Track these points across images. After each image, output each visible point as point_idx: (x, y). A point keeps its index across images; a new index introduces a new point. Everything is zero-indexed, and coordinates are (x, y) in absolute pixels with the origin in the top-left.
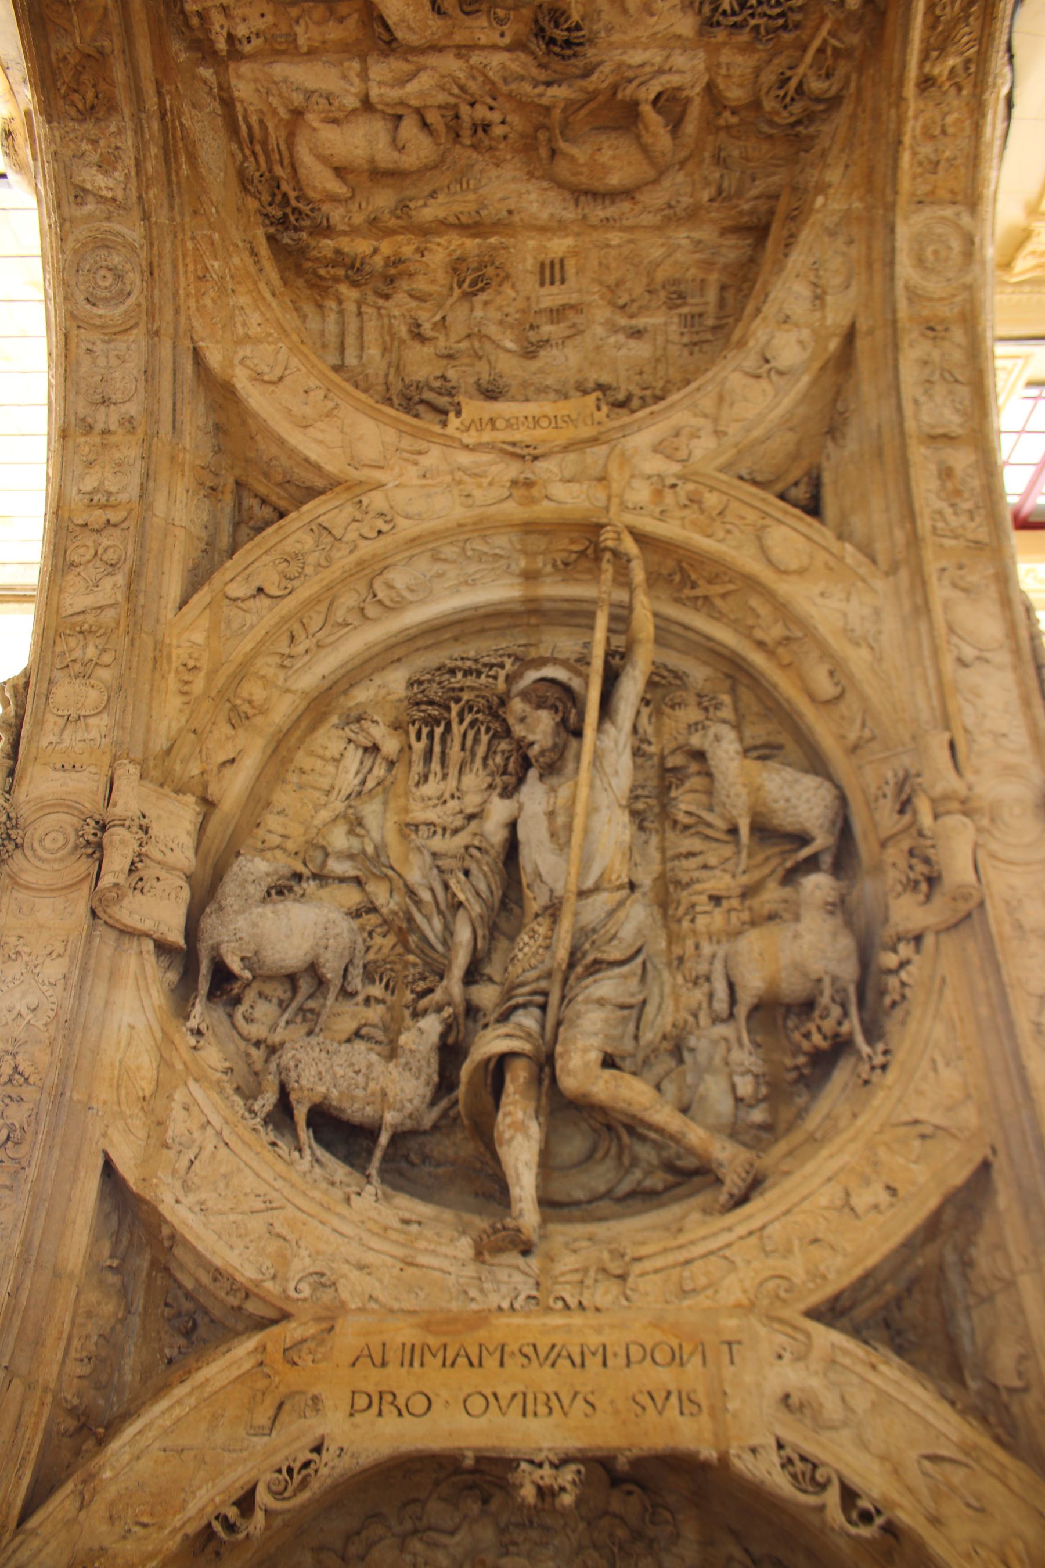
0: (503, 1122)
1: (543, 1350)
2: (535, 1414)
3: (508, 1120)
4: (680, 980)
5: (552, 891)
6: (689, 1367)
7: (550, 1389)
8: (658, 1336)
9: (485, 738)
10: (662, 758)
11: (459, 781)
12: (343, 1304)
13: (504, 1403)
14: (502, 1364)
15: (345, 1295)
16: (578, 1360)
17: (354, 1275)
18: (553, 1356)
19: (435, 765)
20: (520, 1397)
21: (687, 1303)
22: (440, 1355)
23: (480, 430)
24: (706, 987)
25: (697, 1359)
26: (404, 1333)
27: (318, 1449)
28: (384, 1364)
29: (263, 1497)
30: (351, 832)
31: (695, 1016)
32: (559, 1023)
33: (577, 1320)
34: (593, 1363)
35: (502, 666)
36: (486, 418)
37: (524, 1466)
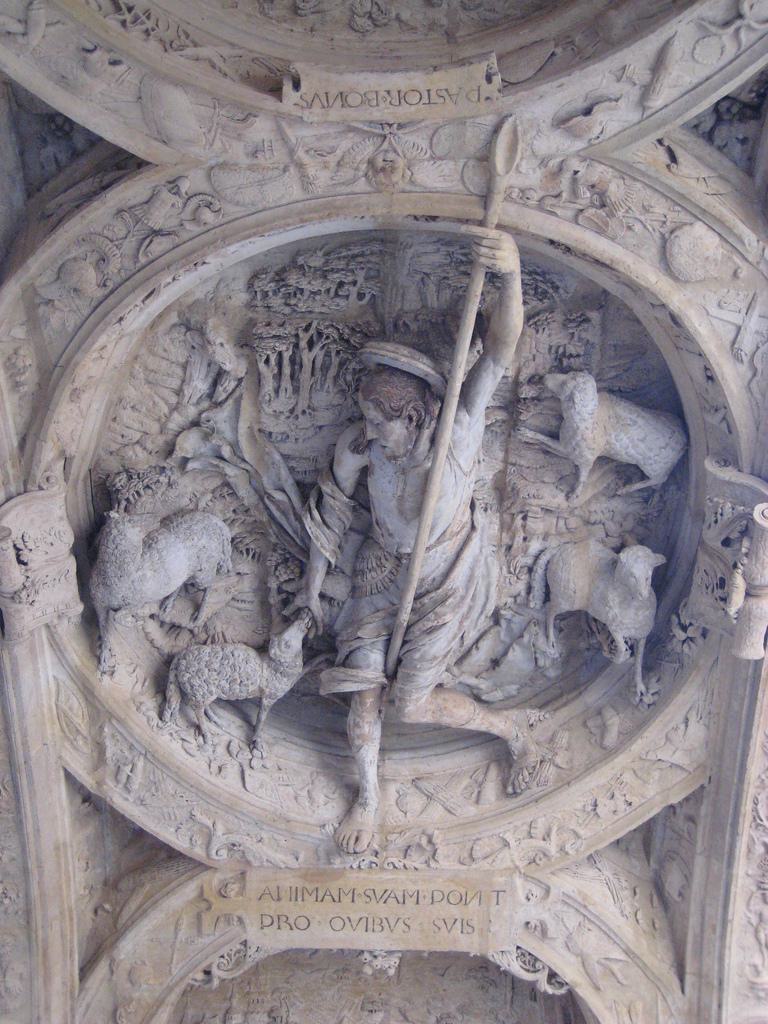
0: (354, 733)
1: (379, 893)
2: (373, 930)
6: (470, 905)
8: (453, 887)
9: (335, 361)
14: (353, 901)
18: (386, 897)
20: (364, 920)
21: (474, 866)
22: (314, 895)
23: (326, 106)
25: (475, 901)
26: (289, 882)
28: (279, 899)
29: (215, 971)
32: (399, 661)
33: (402, 876)
35: (354, 283)
36: (334, 92)
37: (366, 955)
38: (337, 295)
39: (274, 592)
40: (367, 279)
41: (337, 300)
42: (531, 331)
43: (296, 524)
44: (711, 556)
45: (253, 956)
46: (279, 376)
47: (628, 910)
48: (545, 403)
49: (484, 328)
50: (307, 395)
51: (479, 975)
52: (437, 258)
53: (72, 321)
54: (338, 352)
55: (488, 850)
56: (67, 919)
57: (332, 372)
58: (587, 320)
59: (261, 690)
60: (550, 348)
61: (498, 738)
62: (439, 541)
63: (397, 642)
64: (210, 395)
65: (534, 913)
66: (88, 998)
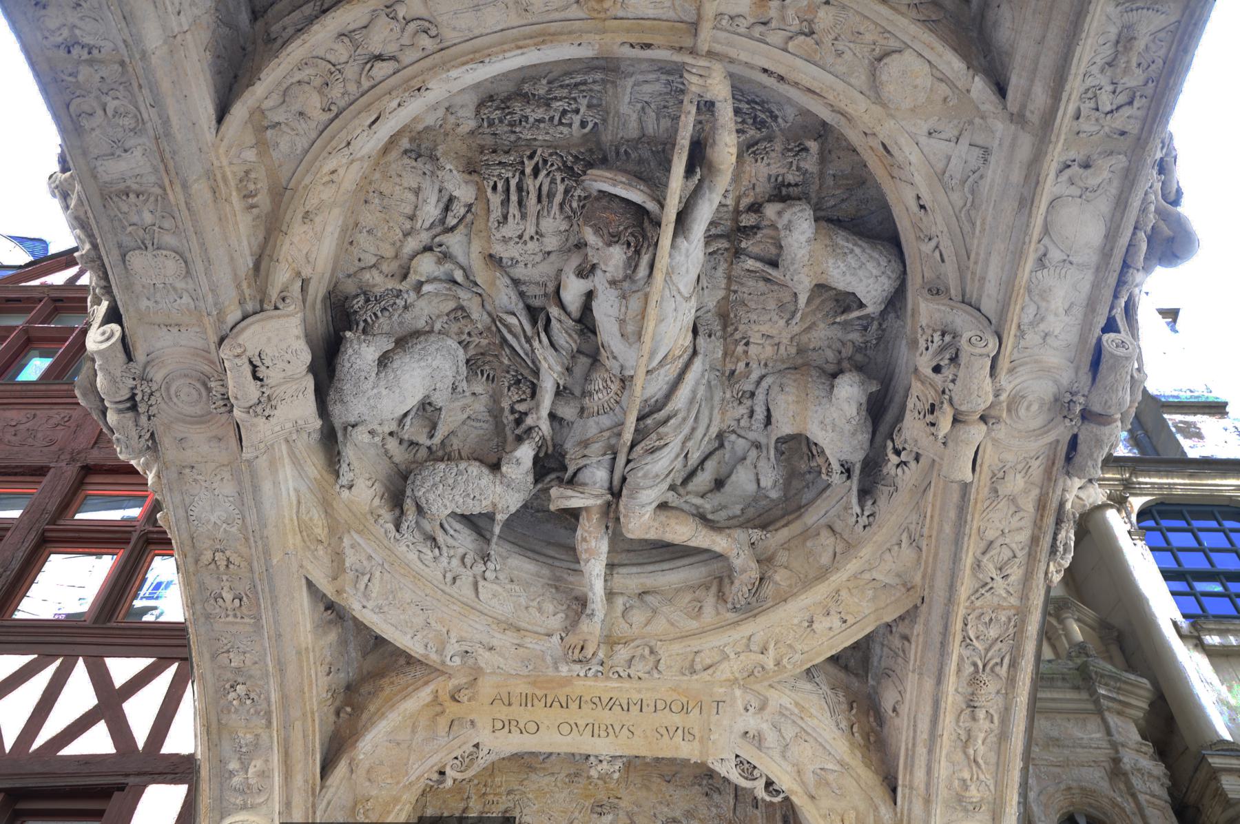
0: (581, 547)
3: (585, 546)
4: (728, 395)
5: (622, 367)
7: (608, 723)
8: (675, 696)
10: (737, 212)
11: (538, 224)
12: (480, 668)
13: (581, 729)
15: (483, 665)
16: (625, 707)
17: (487, 654)
18: (611, 704)
19: (513, 209)
21: (695, 677)
24: (748, 403)
25: (697, 710)
26: (521, 688)
27: (477, 746)
28: (510, 705)
30: (439, 262)
31: (739, 421)
33: (627, 685)
34: (635, 709)
35: (577, 111)
37: (592, 759)
38: (560, 123)
39: (507, 413)
40: (589, 106)
41: (561, 128)
42: (749, 159)
43: (527, 346)
44: (923, 383)
45: (483, 761)
46: (506, 202)
47: (844, 724)
48: (764, 231)
49: (699, 156)
50: (534, 221)
51: (705, 782)
52: (658, 87)
53: (302, 143)
54: (563, 180)
55: (708, 662)
56: (310, 720)
57: (559, 198)
58: (806, 150)
59: (494, 505)
60: (770, 176)
61: (721, 555)
62: (661, 364)
63: (621, 460)
64: (443, 221)
65: (752, 722)
66: (329, 795)
